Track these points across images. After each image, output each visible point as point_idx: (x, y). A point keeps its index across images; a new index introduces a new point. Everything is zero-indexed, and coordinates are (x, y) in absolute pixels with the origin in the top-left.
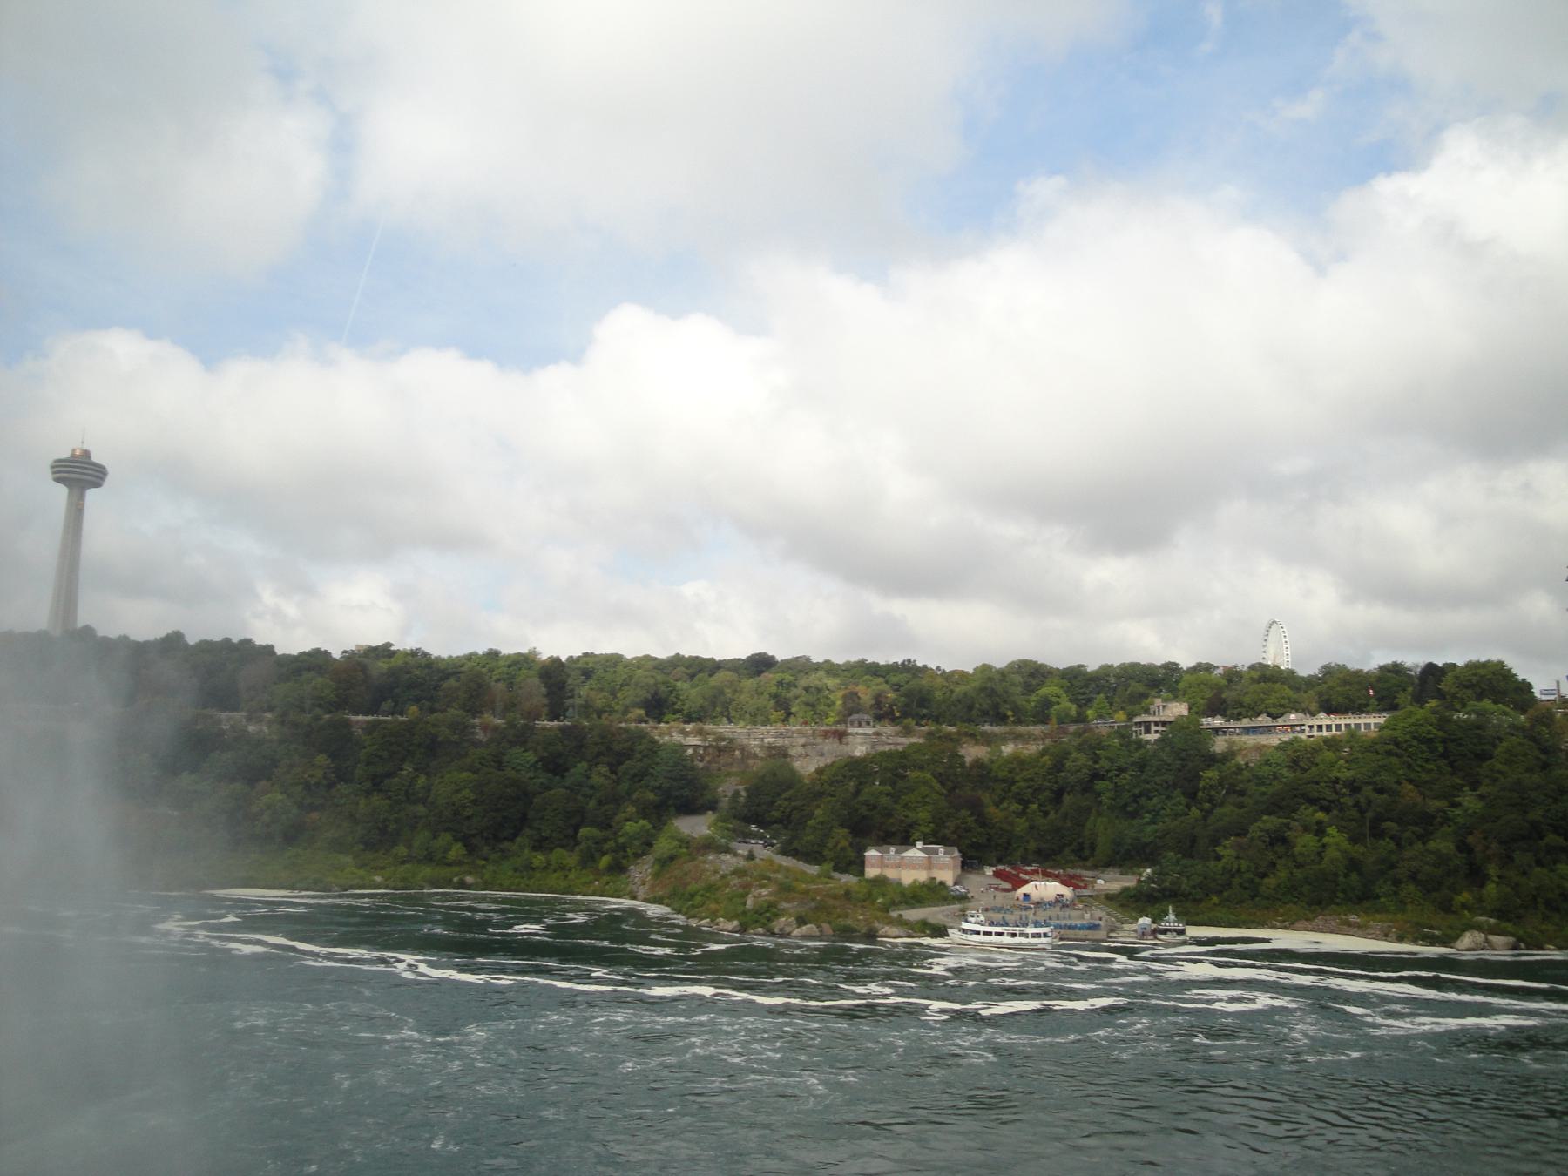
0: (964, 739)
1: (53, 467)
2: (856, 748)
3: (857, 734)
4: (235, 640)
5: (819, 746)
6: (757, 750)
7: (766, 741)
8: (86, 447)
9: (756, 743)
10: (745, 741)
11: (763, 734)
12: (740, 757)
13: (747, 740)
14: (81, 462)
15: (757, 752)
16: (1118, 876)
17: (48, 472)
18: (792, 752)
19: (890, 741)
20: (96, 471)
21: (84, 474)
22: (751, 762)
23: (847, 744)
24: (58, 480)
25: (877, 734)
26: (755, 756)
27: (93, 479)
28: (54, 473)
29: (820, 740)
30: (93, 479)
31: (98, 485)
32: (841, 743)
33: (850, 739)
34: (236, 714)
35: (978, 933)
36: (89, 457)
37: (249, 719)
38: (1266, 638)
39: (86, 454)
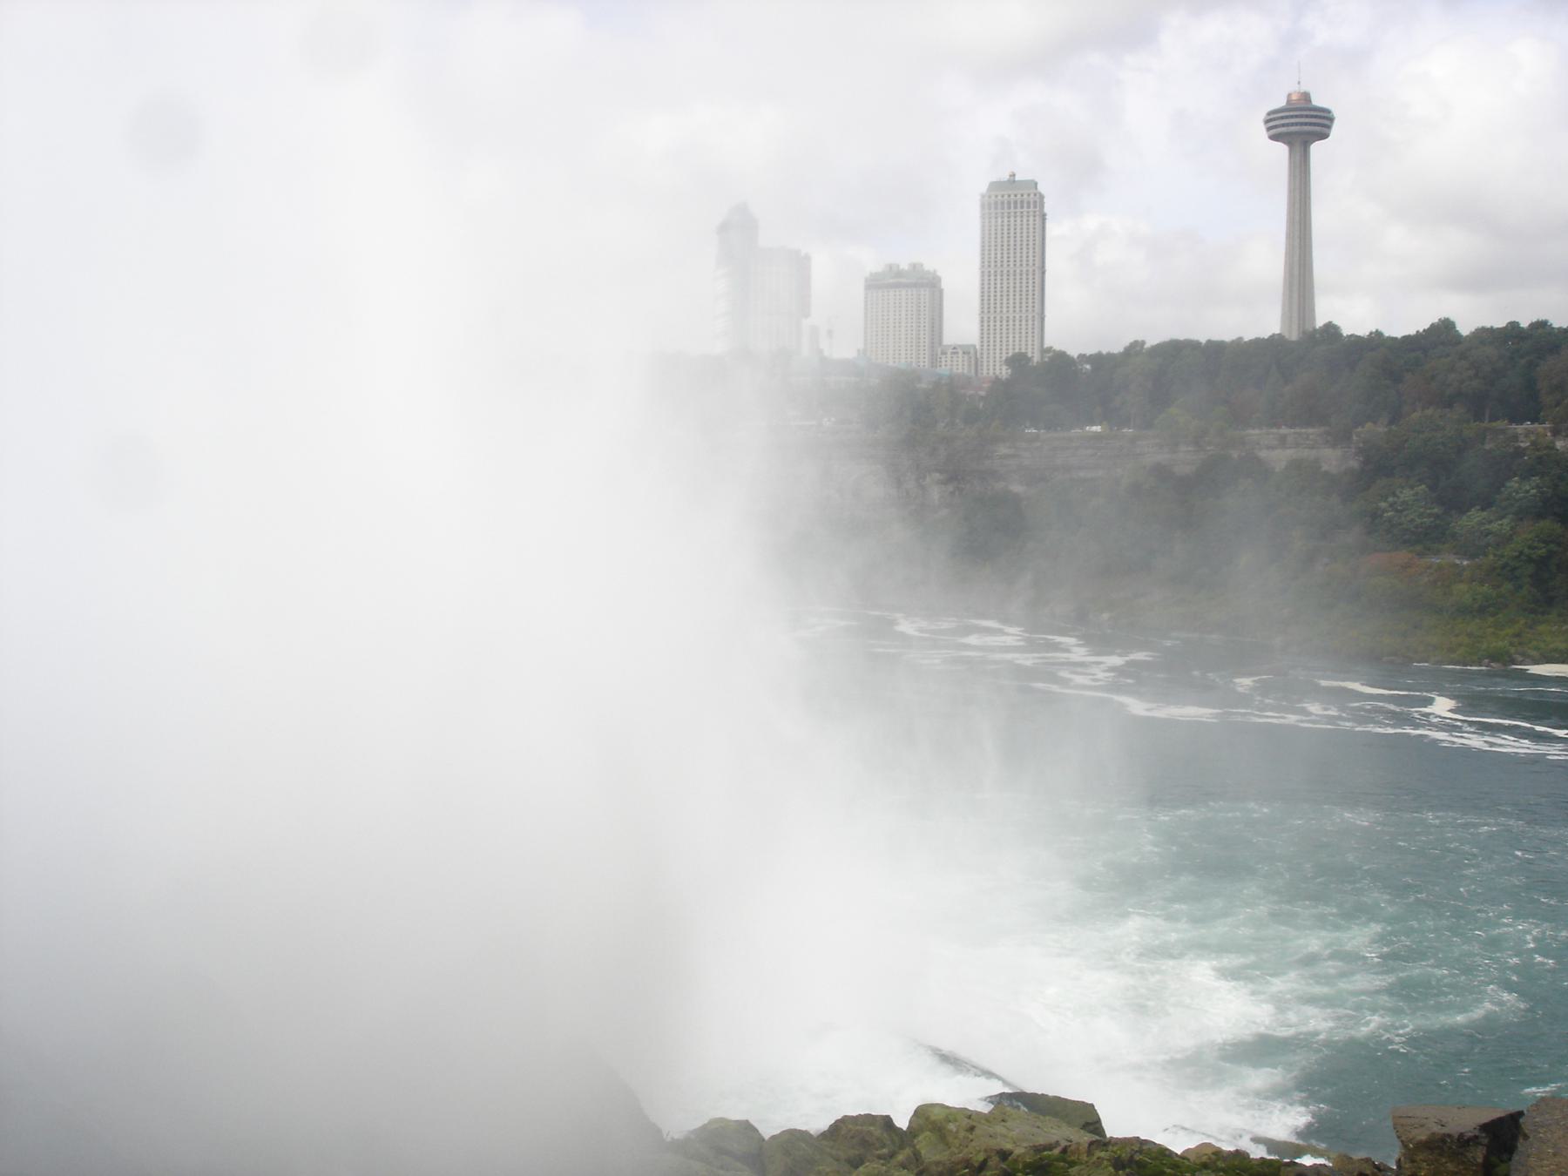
1: (1267, 122)
4: (1524, 324)
8: (1304, 88)
14: (1301, 109)
17: (1262, 128)
20: (1320, 117)
21: (1306, 124)
24: (1274, 138)
27: (1317, 129)
28: (1269, 129)
30: (1317, 129)
31: (1324, 136)
34: (1536, 425)
36: (1310, 101)
37: (1556, 432)
39: (1306, 97)
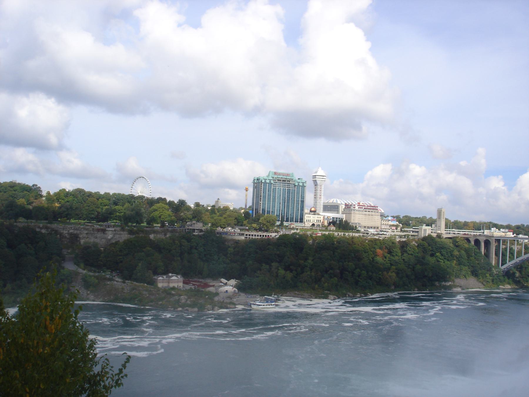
0: (140, 233)
2: (109, 236)
3: (110, 230)
5: (95, 235)
6: (67, 235)
7: (70, 231)
9: (66, 232)
10: (62, 231)
11: (69, 229)
12: (59, 238)
13: (62, 231)
15: (66, 236)
16: (211, 281)
18: (81, 236)
19: (118, 233)
22: (63, 240)
23: (106, 234)
25: (115, 230)
26: (66, 237)
29: (96, 232)
32: (104, 234)
33: (107, 232)
35: (262, 305)
38: (134, 182)
